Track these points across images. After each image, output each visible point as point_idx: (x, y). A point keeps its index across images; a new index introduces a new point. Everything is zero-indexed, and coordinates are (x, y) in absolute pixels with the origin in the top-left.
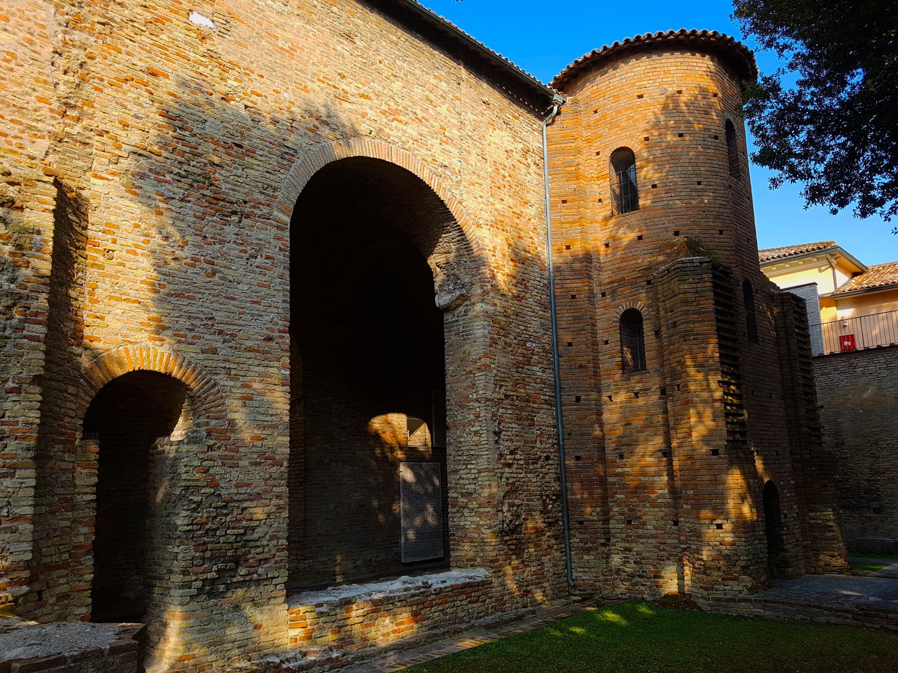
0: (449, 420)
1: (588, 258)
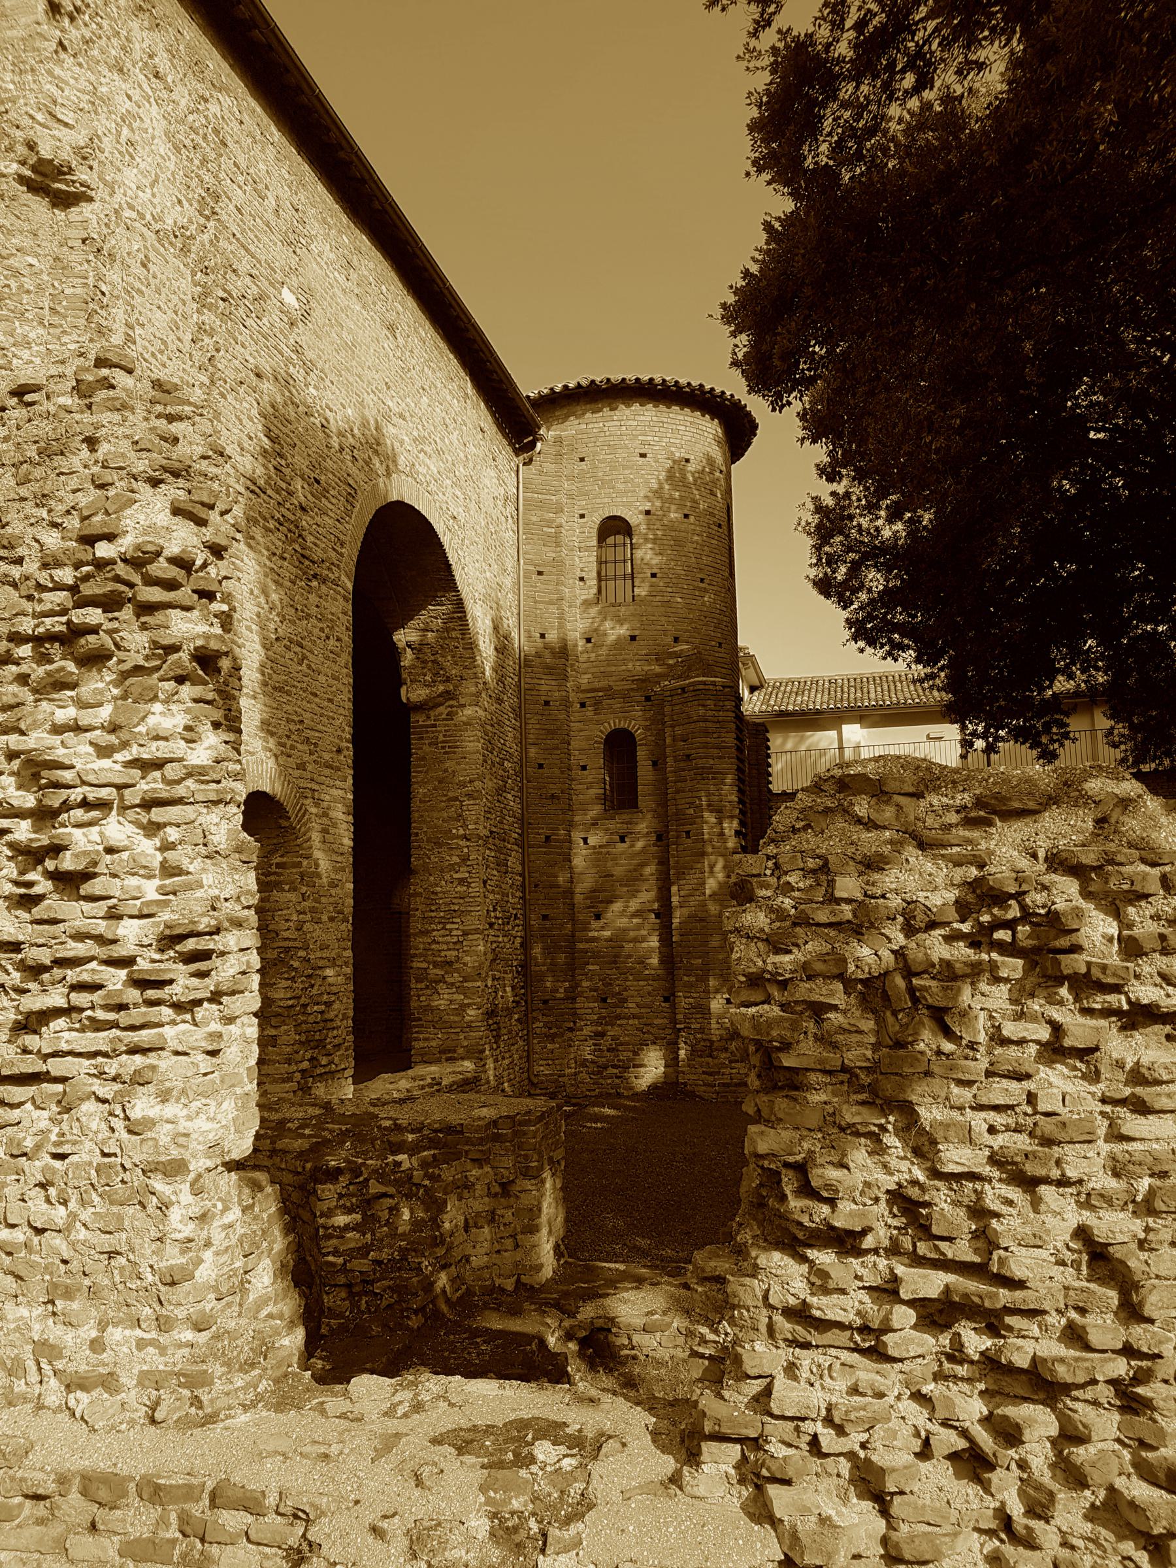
1: (563, 651)
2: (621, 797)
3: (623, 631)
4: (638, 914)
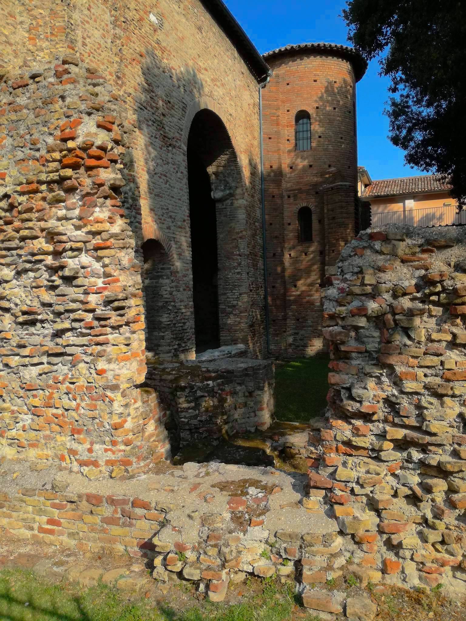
0: (219, 265)
2: (305, 236)
3: (306, 163)
4: (312, 285)
